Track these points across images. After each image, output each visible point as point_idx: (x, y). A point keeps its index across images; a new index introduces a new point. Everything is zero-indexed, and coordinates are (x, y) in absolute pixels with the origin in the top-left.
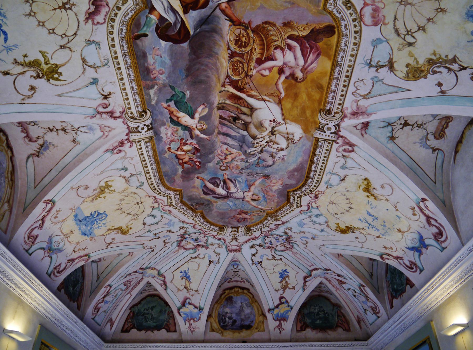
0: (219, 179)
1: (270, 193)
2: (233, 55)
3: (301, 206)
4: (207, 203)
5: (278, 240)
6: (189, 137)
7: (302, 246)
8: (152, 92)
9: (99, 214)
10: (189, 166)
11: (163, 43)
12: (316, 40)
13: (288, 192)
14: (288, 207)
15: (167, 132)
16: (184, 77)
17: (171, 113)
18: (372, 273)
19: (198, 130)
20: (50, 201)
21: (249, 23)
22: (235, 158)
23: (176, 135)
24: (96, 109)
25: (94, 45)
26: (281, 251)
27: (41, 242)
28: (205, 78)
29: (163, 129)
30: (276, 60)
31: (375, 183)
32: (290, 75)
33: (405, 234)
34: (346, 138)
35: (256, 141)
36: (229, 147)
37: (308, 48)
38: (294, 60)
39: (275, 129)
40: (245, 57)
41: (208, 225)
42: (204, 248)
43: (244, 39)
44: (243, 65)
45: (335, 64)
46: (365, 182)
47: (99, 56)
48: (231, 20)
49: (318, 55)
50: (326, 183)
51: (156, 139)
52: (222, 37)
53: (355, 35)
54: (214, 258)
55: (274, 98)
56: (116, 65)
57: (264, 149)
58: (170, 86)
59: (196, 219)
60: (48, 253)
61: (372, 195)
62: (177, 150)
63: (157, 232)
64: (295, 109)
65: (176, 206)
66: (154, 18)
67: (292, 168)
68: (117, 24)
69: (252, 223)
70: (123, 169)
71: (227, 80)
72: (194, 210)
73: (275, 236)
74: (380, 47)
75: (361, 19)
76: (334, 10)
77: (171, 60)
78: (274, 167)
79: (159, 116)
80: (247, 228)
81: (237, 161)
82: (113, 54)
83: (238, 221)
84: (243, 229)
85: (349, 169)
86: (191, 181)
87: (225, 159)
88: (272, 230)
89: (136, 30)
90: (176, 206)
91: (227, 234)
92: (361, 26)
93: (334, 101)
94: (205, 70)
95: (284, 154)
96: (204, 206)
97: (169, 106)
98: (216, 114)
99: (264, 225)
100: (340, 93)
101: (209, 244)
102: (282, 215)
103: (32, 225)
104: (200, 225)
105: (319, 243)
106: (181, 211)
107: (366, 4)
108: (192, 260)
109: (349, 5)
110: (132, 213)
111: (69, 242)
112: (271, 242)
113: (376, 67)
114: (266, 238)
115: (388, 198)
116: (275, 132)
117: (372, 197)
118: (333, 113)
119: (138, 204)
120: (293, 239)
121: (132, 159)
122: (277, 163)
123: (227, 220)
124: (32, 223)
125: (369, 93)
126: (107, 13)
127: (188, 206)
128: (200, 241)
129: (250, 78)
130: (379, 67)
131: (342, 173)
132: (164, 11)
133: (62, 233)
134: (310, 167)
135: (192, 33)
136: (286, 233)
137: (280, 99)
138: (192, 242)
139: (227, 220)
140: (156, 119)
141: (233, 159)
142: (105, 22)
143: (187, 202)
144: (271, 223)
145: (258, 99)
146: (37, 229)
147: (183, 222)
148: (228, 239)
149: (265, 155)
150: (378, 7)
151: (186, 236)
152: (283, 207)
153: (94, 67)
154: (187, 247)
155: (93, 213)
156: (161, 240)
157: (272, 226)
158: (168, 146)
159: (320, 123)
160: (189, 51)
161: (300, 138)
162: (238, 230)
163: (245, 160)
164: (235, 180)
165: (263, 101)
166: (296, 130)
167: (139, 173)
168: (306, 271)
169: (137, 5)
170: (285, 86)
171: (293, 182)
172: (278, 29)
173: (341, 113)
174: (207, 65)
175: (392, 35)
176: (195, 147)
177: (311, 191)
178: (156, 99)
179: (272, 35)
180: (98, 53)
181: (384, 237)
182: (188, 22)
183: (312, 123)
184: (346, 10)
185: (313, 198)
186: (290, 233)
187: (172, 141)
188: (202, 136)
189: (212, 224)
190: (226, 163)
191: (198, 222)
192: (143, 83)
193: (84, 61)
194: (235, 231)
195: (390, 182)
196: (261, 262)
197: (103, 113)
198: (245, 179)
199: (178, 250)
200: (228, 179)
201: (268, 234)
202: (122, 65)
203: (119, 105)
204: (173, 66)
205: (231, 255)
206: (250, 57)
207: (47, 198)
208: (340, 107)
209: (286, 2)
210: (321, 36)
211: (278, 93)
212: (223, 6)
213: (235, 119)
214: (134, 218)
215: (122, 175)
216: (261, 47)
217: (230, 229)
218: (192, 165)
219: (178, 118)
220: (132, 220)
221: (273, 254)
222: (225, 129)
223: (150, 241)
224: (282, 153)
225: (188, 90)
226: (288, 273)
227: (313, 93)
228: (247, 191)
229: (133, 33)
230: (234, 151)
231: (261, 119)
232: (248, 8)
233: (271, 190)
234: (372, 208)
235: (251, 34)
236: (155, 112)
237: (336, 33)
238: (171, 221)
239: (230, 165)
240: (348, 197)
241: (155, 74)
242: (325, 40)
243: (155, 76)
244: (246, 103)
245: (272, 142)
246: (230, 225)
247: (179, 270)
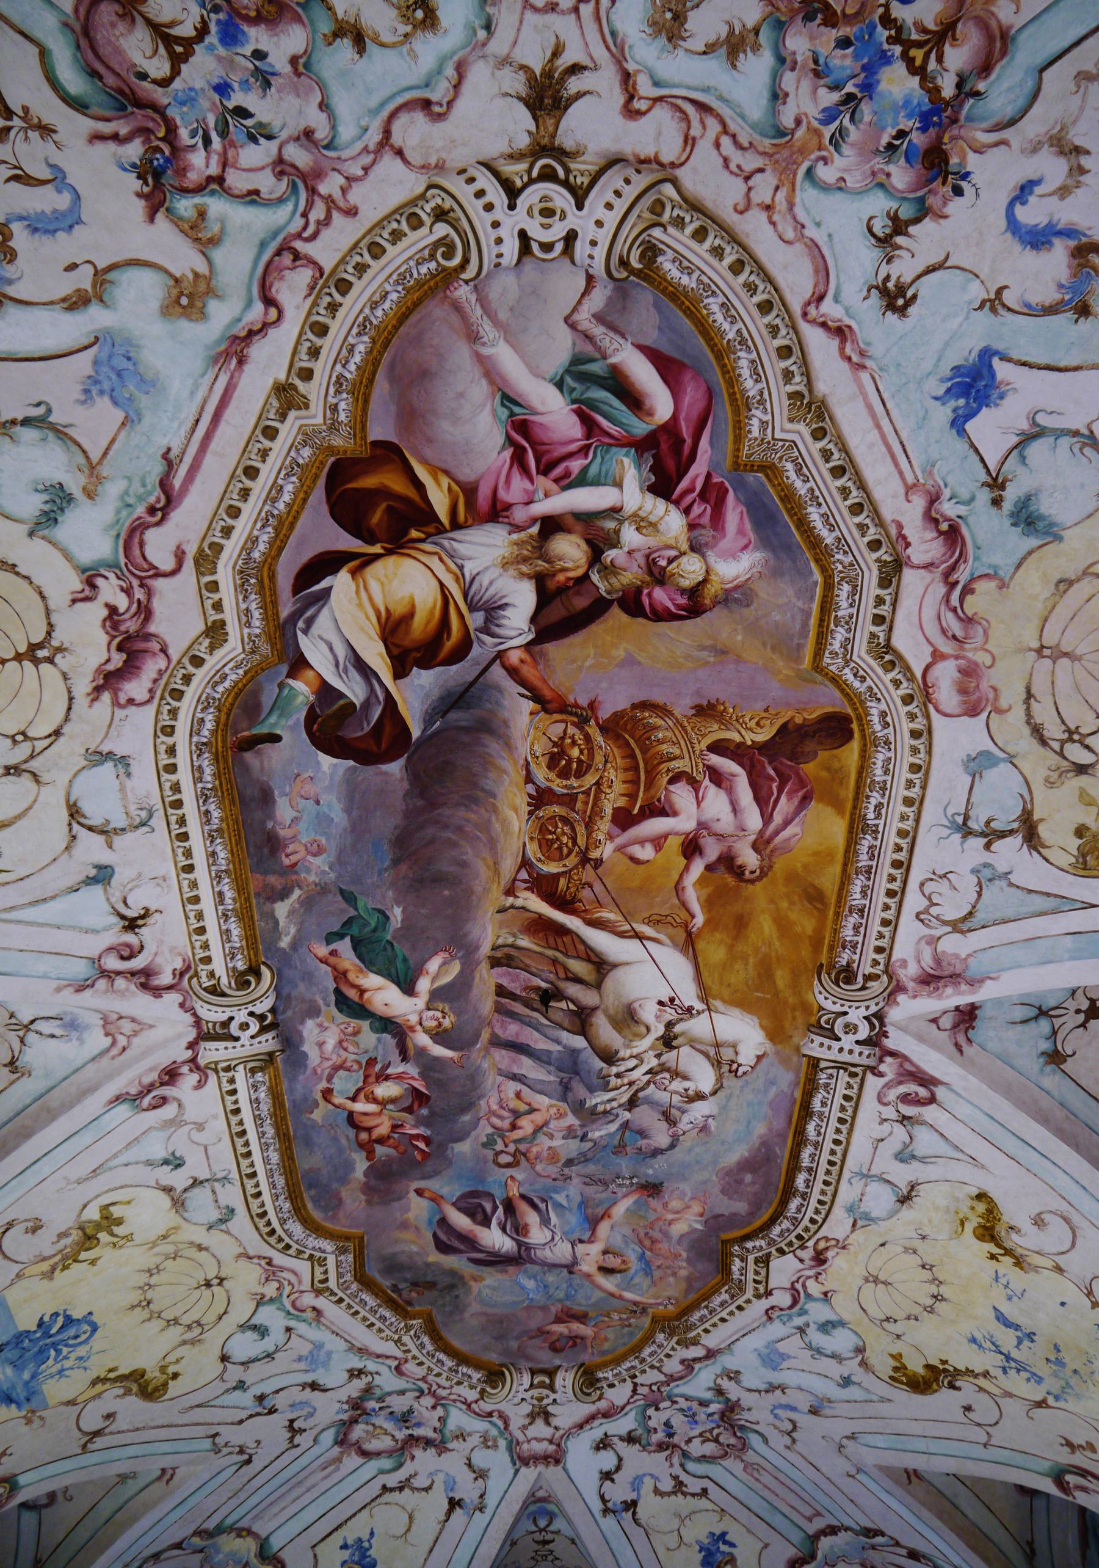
0: (491, 1197)
1: (664, 1246)
2: (541, 798)
3: (768, 1293)
4: (446, 1280)
5: (692, 1418)
6: (394, 1056)
7: (779, 1441)
8: (281, 910)
10: (392, 1151)
11: (326, 761)
12: (796, 757)
13: (725, 1243)
14: (725, 1297)
15: (323, 1037)
16: (387, 864)
17: (341, 976)
18: (1030, 1544)
19: (427, 1031)
21: (592, 706)
22: (546, 1124)
23: (351, 1048)
25: (110, 764)
26: (703, 1459)
28: (453, 869)
29: (309, 1029)
30: (675, 814)
31: (1015, 1211)
32: (720, 859)
34: (906, 1058)
35: (614, 1070)
36: (525, 1089)
37: (772, 780)
38: (731, 816)
39: (677, 1029)
40: (579, 805)
41: (449, 1363)
42: (432, 1452)
43: (575, 752)
44: (573, 829)
45: (857, 827)
46: (981, 1207)
47: (124, 798)
48: (536, 697)
49: (805, 800)
50: (850, 1209)
51: (285, 1061)
52: (508, 746)
53: (914, 742)
54: (468, 1490)
55: (670, 930)
56: (174, 826)
58: (342, 891)
59: (406, 1339)
62: (354, 1099)
63: (267, 1388)
65: (340, 1294)
66: (302, 689)
67: (735, 1156)
68: (187, 707)
69: (603, 1353)
70: (166, 1162)
71: (523, 875)
72: (401, 1309)
73: (683, 1404)
74: (992, 775)
75: (928, 697)
76: (847, 671)
77: (348, 810)
78: (678, 1154)
79: (302, 987)
80: (585, 1373)
81: (551, 1137)
82: (168, 792)
83: (555, 1349)
84: (570, 1377)
85: (923, 1160)
86: (396, 1205)
87: (514, 1127)
88: (671, 1378)
89: (244, 725)
90: (340, 1294)
91: (515, 1397)
92: (928, 716)
93: (860, 939)
94: (454, 845)
95: (707, 1112)
96: (435, 1293)
97: (334, 953)
98: (487, 979)
99: (643, 1361)
100: (877, 915)
101: (448, 1434)
102: (707, 1326)
104: (421, 1364)
105: (840, 1428)
106: (357, 1313)
107: (937, 656)
108: (388, 1497)
109: (888, 657)
110: (186, 1320)
112: (667, 1424)
113: (983, 834)
114: (651, 1412)
116: (676, 1037)
118: (860, 979)
119: (208, 1285)
120: (746, 1415)
121: (200, 1127)
122: (686, 1143)
123: (514, 1345)
125: (971, 913)
126: (161, 673)
127: (384, 1292)
128: (419, 1425)
129: (596, 868)
130: (992, 836)
131: (902, 1174)
132: (333, 669)
134: (795, 1156)
135: (416, 733)
136: (719, 1392)
137: (689, 934)
138: (389, 1426)
139: (514, 1345)
140: (289, 996)
141: (538, 1129)
142: (152, 698)
143: (378, 1277)
144: (668, 1356)
145: (621, 935)
147: (362, 1351)
148: (518, 1415)
149: (644, 1116)
150: (976, 664)
151: (372, 1404)
152: (707, 1297)
153: (103, 832)
154: (373, 1445)
156: (279, 1420)
157: (673, 1366)
158: (324, 1085)
159: (821, 1008)
160: (406, 785)
161: (759, 1058)
162: (552, 1381)
163: (580, 1133)
164: (544, 1200)
165: (636, 942)
166: (743, 1033)
167: (220, 1175)
168: (796, 1537)
169: (253, 652)
171: (741, 1207)
172: (678, 722)
173: (885, 978)
174: (460, 829)
175: (1025, 743)
176: (415, 1089)
177: (799, 1237)
178: (293, 930)
179: (660, 742)
180: (122, 789)
182: (405, 701)
183: (794, 1009)
184: (880, 671)
185: (808, 1263)
186: (733, 1392)
187: (336, 1068)
188: (439, 1051)
189: (462, 1359)
190: (515, 1142)
191: (415, 1352)
192: (254, 883)
193: (74, 812)
194: (542, 1385)
196: (634, 1503)
197: (118, 973)
198: (578, 1199)
199: (339, 1460)
200: (523, 1197)
201: (657, 1395)
202: (194, 827)
203: (172, 949)
204: (352, 831)
205: (529, 1474)
206: (595, 804)
208: (881, 958)
209: (702, 648)
210: (810, 746)
211: (684, 915)
212: (514, 657)
213: (547, 997)
214: (189, 1336)
215: (164, 1182)
216: (630, 775)
217: (526, 1379)
218: (402, 1148)
219: (362, 991)
220: (184, 1343)
221: (677, 1470)
222: (512, 1030)
223: (241, 1422)
224: (700, 1110)
225: (398, 904)
226: (732, 1545)
227: (793, 916)
228: (586, 1237)
229: (236, 733)
231: (632, 997)
232: (588, 663)
233: (666, 1234)
235: (599, 739)
236: (288, 973)
237: (856, 735)
238: (318, 1346)
240: (929, 1260)
241: (294, 853)
242: (823, 755)
243: (294, 859)
244: (581, 947)
245: (668, 1070)
246: (524, 1364)
247: (337, 1539)
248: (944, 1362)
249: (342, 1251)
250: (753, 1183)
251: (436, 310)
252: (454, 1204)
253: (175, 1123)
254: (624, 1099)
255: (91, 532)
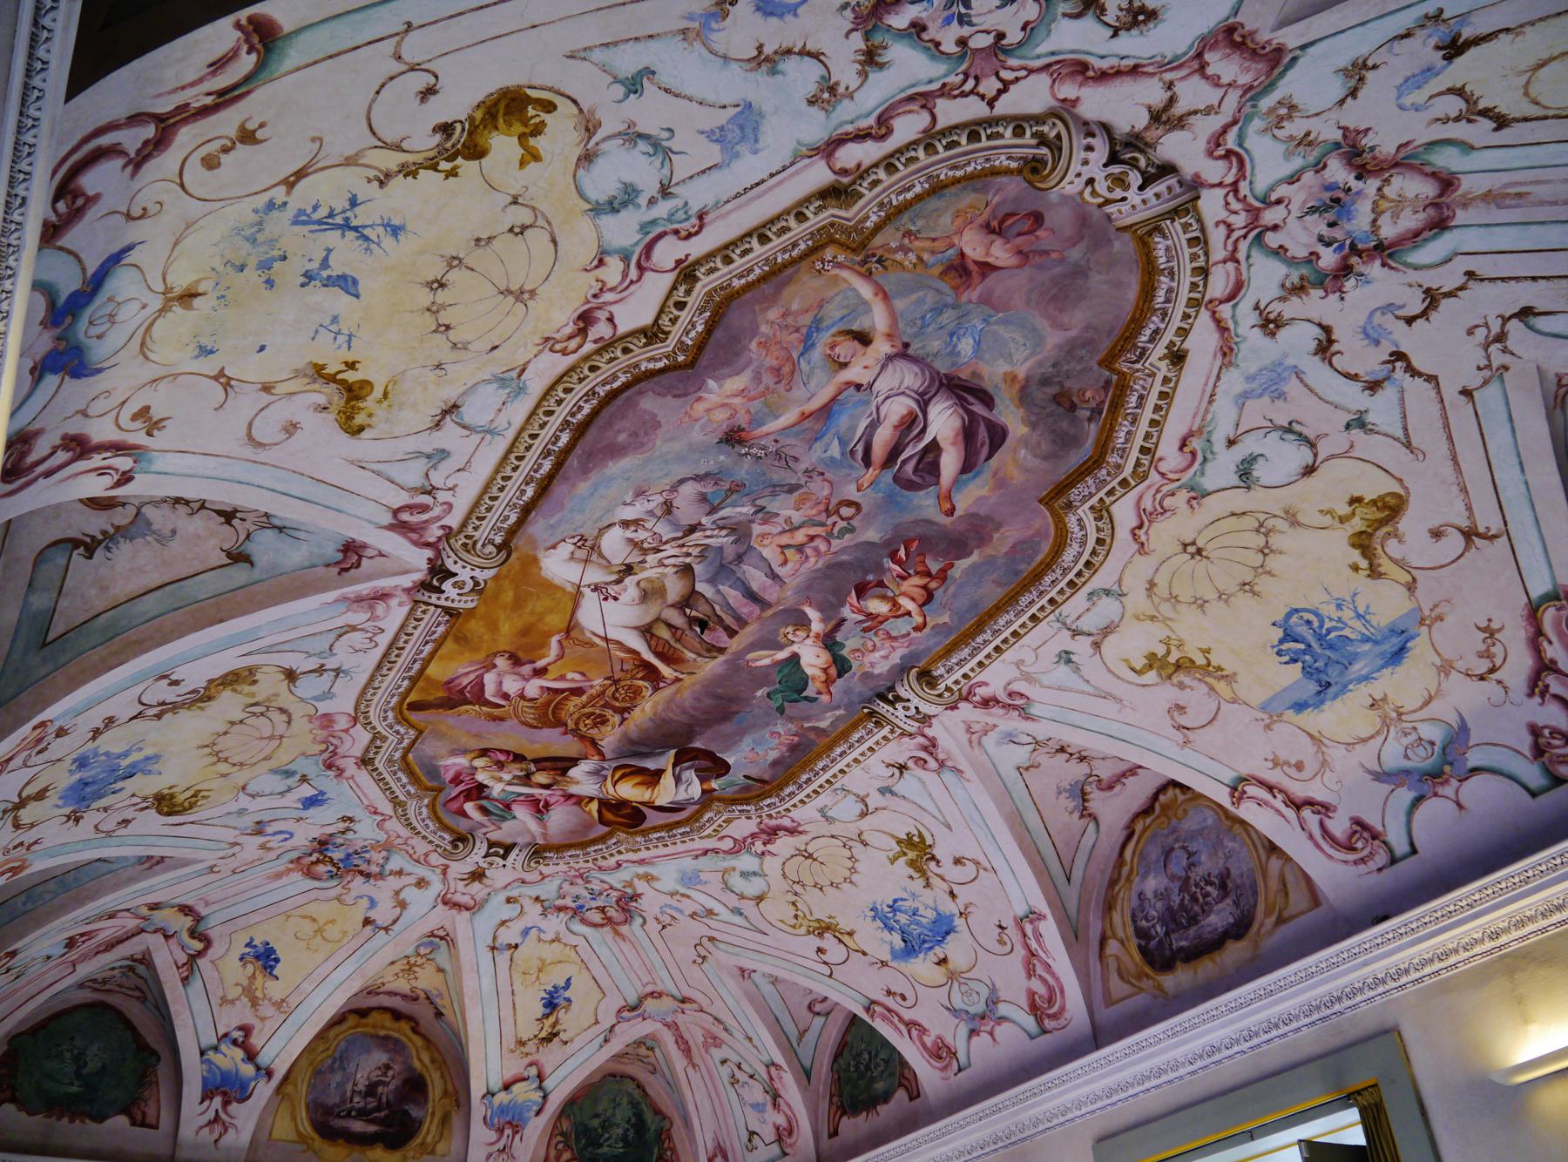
0: (896, 479)
8: (823, 724)
9: (1289, 636)
11: (731, 761)
15: (880, 660)
17: (828, 682)
20: (1234, 789)
22: (783, 532)
24: (938, 772)
27: (1389, 812)
29: (882, 668)
31: (321, 431)
33: (156, 303)
34: (415, 543)
35: (688, 560)
46: (360, 419)
50: (521, 390)
57: (680, 534)
60: (1447, 782)
61: (332, 379)
62: (909, 614)
64: (539, 609)
70: (1069, 661)
78: (681, 471)
85: (420, 454)
87: (812, 538)
94: (694, 709)
103: (1311, 837)
111: (1426, 704)
114: (1014, 36)
115: (265, 398)
117: (330, 370)
119: (1199, 552)
122: (666, 483)
124: (1303, 836)
131: (450, 436)
133: (1372, 737)
135: (673, 752)
143: (1089, 443)
146: (1328, 822)
147: (1227, 352)
149: (687, 510)
155: (1287, 658)
158: (914, 634)
161: (554, 547)
163: (760, 515)
166: (559, 566)
170: (544, 651)
176: (858, 598)
181: (262, 200)
185: (602, 315)
187: (891, 638)
188: (813, 614)
189: (1150, 272)
190: (823, 525)
193: (863, 815)
195: (262, 456)
198: (817, 445)
205: (1290, 37)
207: (1225, 801)
208: (419, 614)
211: (565, 643)
219: (825, 670)
224: (629, 513)
227: (483, 630)
228: (852, 390)
230: (767, 553)
233: (757, 377)
234: (335, 319)
239: (820, 513)
240: (440, 338)
248: (453, 173)
249: (1069, 506)
250: (619, 431)
251: (556, 841)
252: (937, 483)
253: (1028, 678)
254: (697, 535)
255: (747, 862)
